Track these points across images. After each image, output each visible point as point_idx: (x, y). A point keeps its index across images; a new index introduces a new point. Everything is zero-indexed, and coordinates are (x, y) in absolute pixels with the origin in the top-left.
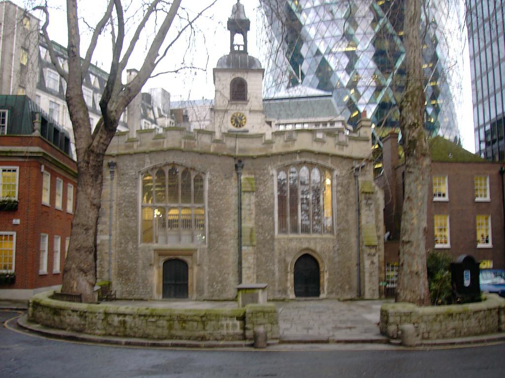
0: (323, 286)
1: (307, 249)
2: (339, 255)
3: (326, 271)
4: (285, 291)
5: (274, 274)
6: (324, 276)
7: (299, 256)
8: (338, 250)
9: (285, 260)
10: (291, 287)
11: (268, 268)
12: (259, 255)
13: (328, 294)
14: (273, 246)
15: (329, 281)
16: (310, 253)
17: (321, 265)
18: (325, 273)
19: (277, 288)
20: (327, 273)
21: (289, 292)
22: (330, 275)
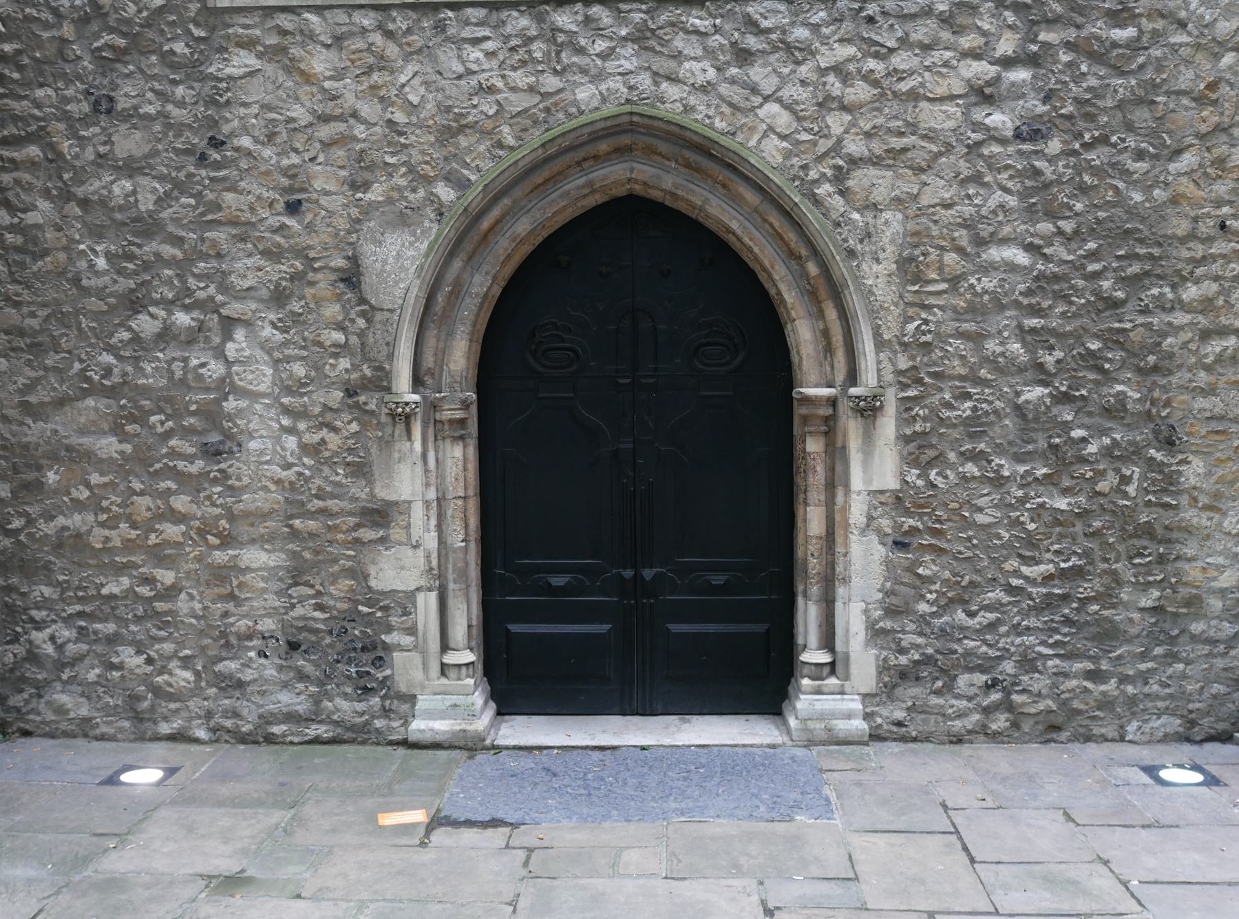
0: (829, 581)
1: (632, 132)
2: (1040, 198)
3: (869, 410)
4: (352, 648)
5: (220, 447)
6: (835, 481)
7: (523, 226)
8: (1030, 132)
9: (351, 278)
10: (427, 604)
11: (150, 375)
12: (42, 211)
13: (894, 679)
14: (217, 99)
15: (914, 526)
16: (664, 180)
17: (803, 335)
18: (852, 428)
19: (262, 610)
20: (888, 426)
21: (407, 668)
22: (918, 449)
